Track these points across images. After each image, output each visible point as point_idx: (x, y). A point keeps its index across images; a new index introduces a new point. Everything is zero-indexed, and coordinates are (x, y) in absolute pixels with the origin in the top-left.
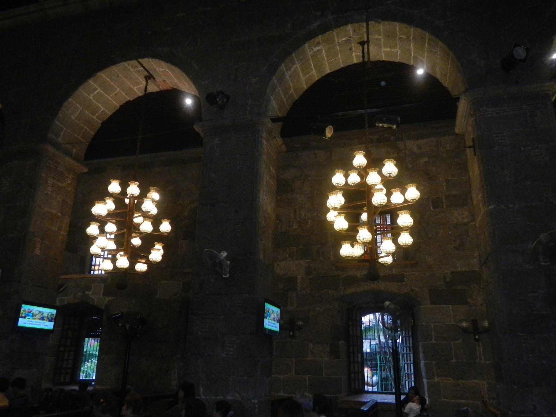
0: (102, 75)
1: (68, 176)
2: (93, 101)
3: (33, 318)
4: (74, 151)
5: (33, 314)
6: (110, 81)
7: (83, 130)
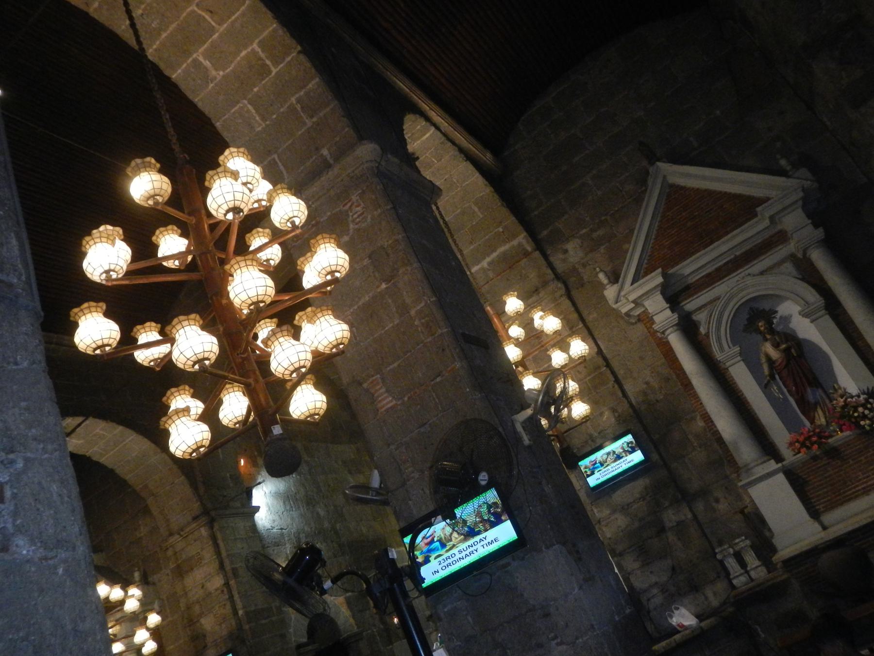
0: (151, 50)
1: (349, 204)
2: (228, 70)
3: (448, 548)
4: (325, 152)
5: (440, 541)
6: (168, 32)
7: (298, 107)
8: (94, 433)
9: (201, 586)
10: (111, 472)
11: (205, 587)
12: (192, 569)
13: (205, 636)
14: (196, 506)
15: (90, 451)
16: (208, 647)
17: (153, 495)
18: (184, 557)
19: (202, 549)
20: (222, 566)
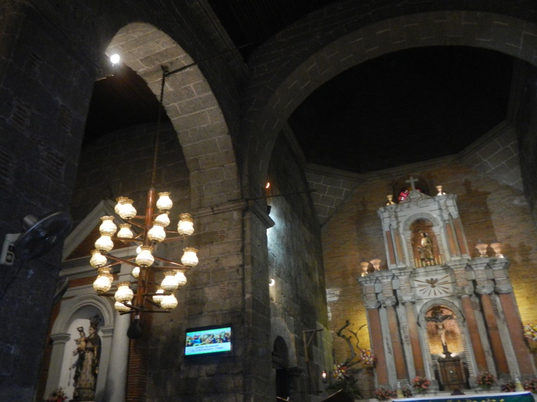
8: (187, 86)
9: (215, 260)
10: (174, 133)
11: (220, 262)
12: (212, 243)
13: (203, 304)
14: (235, 192)
15: (171, 105)
16: (204, 315)
17: (199, 169)
18: (207, 230)
19: (229, 229)
20: (243, 250)
